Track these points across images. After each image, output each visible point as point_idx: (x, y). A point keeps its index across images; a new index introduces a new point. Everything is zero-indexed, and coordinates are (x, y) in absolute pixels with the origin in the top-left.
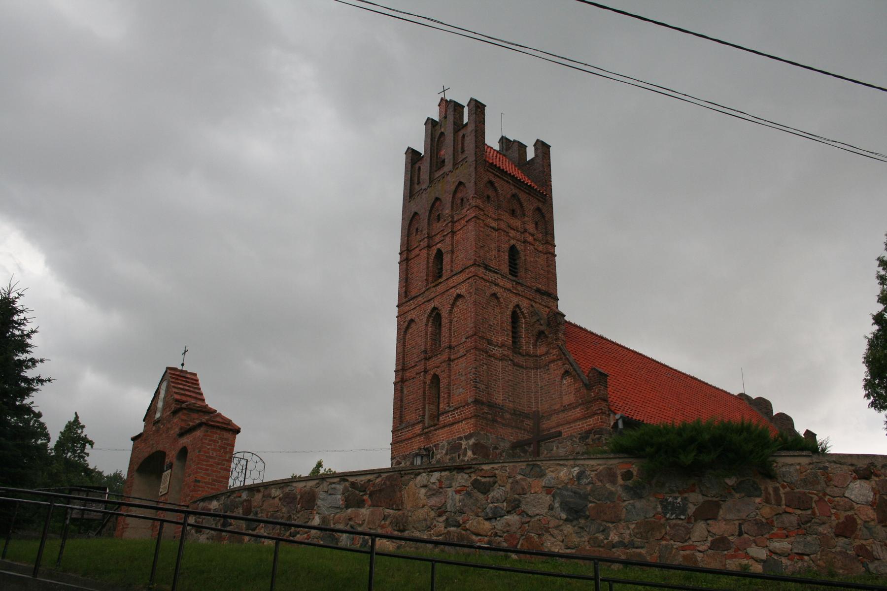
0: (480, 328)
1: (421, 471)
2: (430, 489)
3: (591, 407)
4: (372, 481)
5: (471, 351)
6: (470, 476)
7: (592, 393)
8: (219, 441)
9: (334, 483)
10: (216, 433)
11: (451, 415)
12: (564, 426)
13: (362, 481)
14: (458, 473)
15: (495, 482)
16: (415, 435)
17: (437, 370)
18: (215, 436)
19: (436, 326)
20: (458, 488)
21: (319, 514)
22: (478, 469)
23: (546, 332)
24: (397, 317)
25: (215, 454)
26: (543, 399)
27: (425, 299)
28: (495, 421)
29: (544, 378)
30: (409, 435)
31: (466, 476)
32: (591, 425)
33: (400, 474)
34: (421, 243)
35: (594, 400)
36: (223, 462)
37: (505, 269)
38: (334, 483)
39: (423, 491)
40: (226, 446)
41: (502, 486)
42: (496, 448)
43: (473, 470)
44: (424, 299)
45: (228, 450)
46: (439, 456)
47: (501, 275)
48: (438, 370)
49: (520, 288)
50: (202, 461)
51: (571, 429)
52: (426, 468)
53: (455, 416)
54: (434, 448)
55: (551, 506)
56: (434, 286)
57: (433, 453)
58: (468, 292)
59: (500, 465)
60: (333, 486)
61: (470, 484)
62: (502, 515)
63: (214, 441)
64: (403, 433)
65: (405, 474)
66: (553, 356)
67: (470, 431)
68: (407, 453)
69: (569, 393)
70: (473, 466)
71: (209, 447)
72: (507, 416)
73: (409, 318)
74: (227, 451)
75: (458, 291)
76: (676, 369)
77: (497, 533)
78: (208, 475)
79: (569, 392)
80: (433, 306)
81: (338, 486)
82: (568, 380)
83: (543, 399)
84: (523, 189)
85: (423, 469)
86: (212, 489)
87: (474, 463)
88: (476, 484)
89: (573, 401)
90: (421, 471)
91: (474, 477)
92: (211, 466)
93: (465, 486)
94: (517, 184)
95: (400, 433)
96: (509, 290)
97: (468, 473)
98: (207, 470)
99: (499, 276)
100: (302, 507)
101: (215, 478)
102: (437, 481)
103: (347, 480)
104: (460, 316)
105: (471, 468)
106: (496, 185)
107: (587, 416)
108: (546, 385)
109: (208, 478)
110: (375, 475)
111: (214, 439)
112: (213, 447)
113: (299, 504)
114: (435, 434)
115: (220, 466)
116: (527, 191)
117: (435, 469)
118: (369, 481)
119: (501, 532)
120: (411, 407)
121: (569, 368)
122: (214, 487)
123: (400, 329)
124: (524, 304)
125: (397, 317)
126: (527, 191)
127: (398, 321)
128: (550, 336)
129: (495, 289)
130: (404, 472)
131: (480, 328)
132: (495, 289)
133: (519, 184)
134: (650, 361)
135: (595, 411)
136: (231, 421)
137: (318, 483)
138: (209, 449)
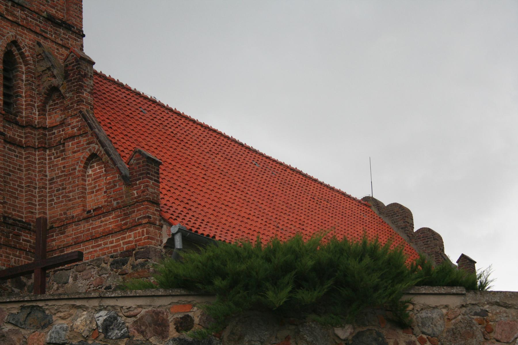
3: (131, 213)
7: (135, 192)
12: (86, 243)
23: (61, 89)
26: (53, 200)
29: (57, 165)
32: (129, 242)
35: (137, 202)
49: (19, 13)
51: (98, 249)
66: (72, 128)
69: (97, 191)
76: (270, 156)
79: (97, 188)
82: (96, 170)
83: (53, 200)
89: (103, 204)
107: (124, 227)
121: (98, 150)
128: (67, 95)
134: (278, 166)
135: (138, 219)
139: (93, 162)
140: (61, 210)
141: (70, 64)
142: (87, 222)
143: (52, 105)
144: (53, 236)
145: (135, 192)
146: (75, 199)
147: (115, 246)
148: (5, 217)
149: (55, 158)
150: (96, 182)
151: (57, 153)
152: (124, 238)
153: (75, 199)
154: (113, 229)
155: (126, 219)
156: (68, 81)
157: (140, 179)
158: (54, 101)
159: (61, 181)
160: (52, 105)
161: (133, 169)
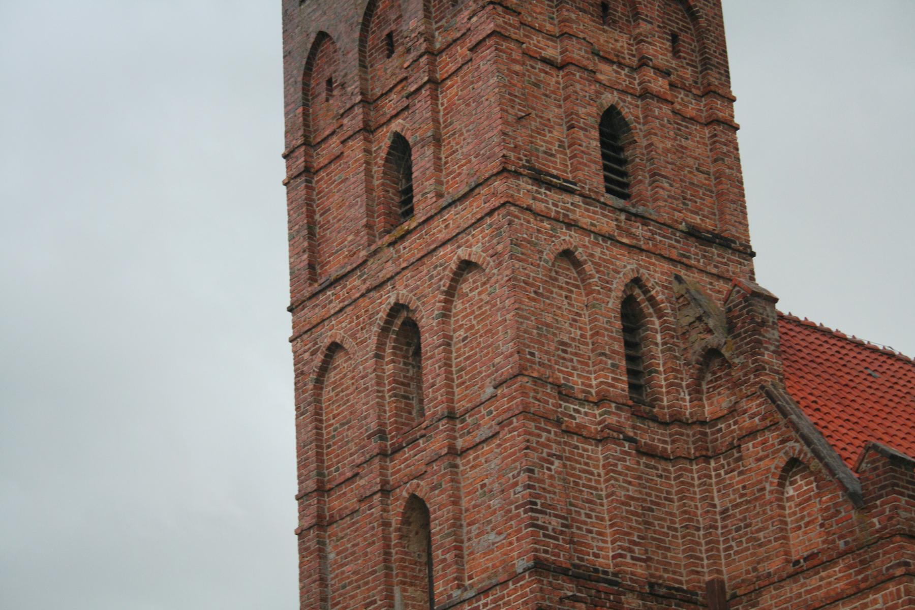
3: (873, 558)
5: (511, 423)
7: (875, 520)
17: (418, 485)
19: (405, 357)
23: (723, 351)
24: (291, 341)
26: (731, 547)
27: (368, 283)
29: (731, 485)
35: (881, 538)
44: (364, 281)
47: (582, 195)
48: (422, 483)
49: (639, 230)
58: (490, 252)
66: (751, 418)
73: (327, 341)
75: (463, 253)
79: (807, 519)
80: (392, 300)
82: (801, 487)
83: (731, 547)
89: (821, 547)
99: (577, 199)
107: (863, 586)
108: (736, 506)
120: (353, 597)
121: (800, 452)
123: (302, 373)
125: (291, 341)
127: (295, 352)
128: (736, 361)
129: (569, 238)
131: (532, 354)
132: (569, 238)
135: (888, 569)
139: (795, 474)
140: (747, 564)
141: (735, 306)
142: (795, 582)
146: (770, 541)
148: (651, 585)
149: (726, 473)
150: (802, 510)
151: (729, 464)
153: (770, 541)
154: (843, 590)
155: (864, 570)
156: (735, 337)
157: (881, 496)
158: (714, 373)
159: (741, 513)
161: (867, 479)
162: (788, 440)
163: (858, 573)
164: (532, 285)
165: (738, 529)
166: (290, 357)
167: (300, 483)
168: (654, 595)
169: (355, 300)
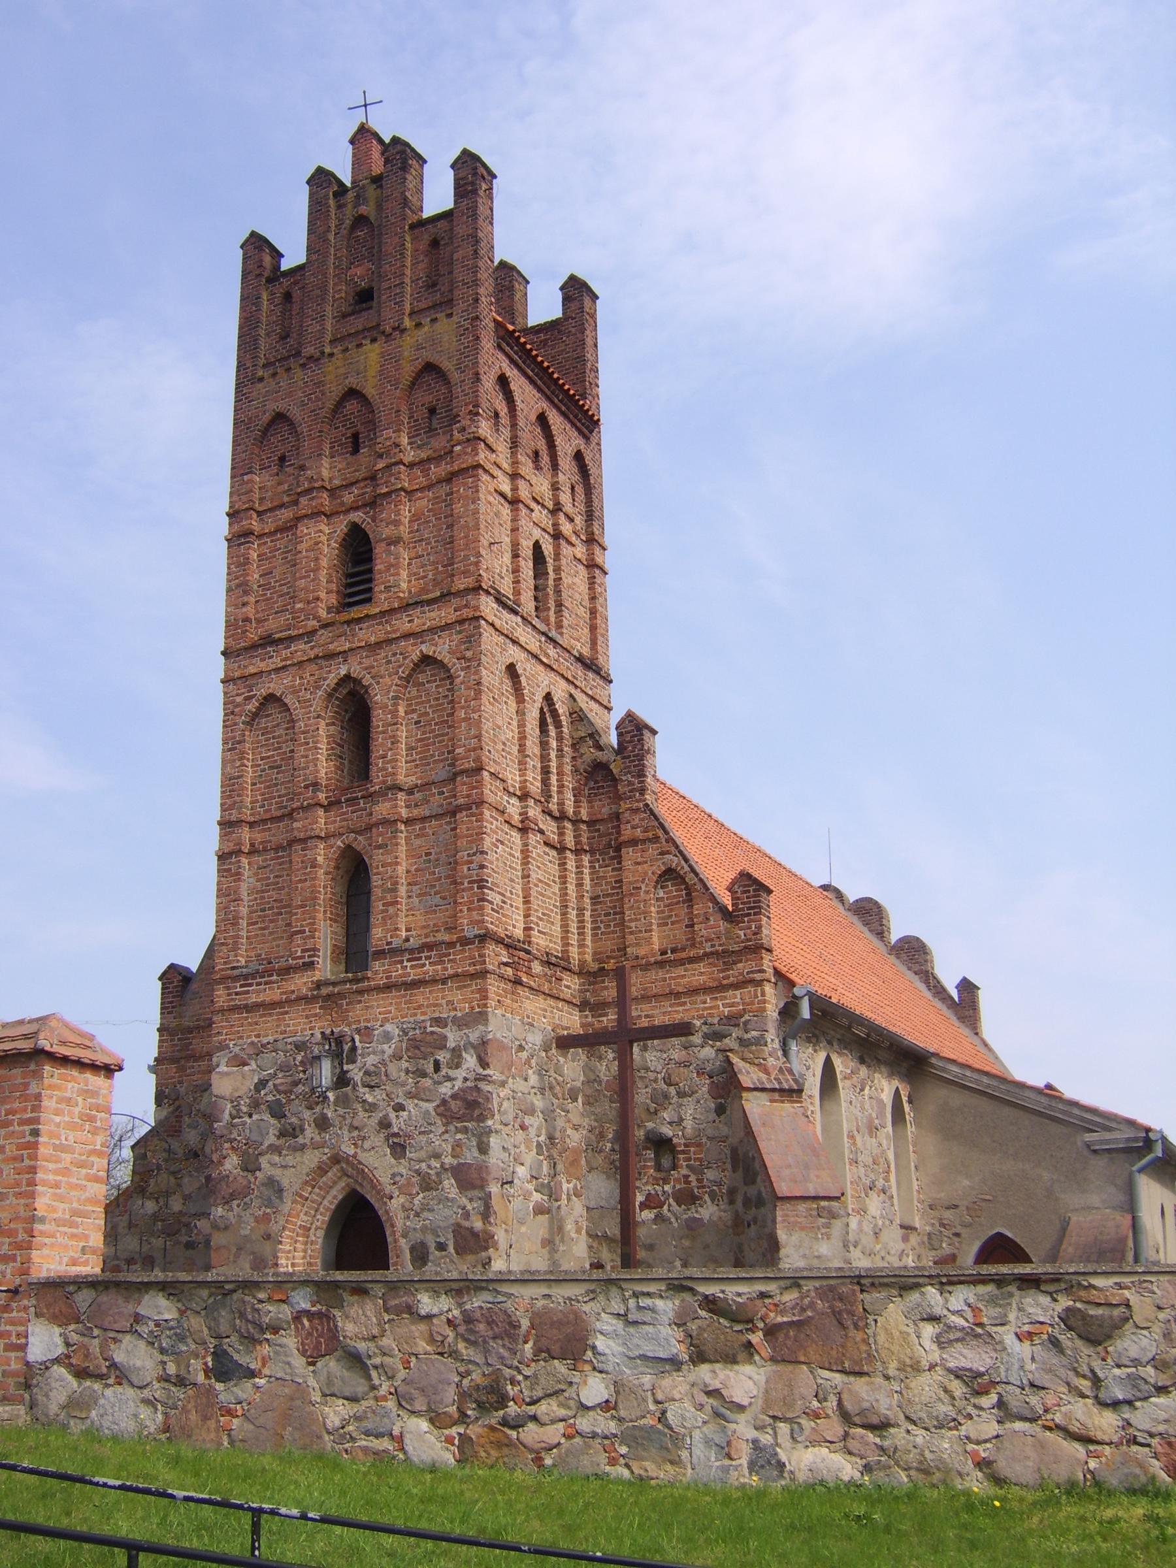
0: (489, 751)
1: (921, 1280)
2: (950, 1328)
3: (735, 963)
4: (770, 1297)
5: (471, 808)
6: (1055, 1300)
7: (742, 933)
8: (80, 1099)
9: (648, 1294)
10: (74, 1079)
11: (408, 960)
12: (661, 998)
13: (739, 1295)
14: (1019, 1289)
15: (1126, 1320)
16: (293, 997)
17: (356, 839)
18: (70, 1085)
19: (342, 721)
20: (1026, 1328)
21: (601, 1372)
22: (1079, 1284)
23: (612, 767)
24: (223, 682)
25: (71, 1138)
26: (599, 928)
27: (316, 651)
28: (518, 982)
29: (605, 878)
30: (273, 994)
31: (1045, 1300)
32: (732, 1005)
33: (858, 1283)
34: (302, 500)
35: (745, 947)
36: (92, 1159)
37: (528, 605)
38: (648, 1294)
39: (929, 1330)
40: (94, 1113)
41: (1142, 1328)
42: (521, 1048)
43: (1063, 1286)
44: (312, 648)
45: (99, 1124)
46: (371, 1060)
47: (522, 617)
48: (360, 838)
49: (552, 651)
50: (47, 1161)
51: (681, 1008)
52: (938, 1276)
53: (424, 965)
54: (357, 1038)
55: (1071, 1322)
56: (348, 622)
57: (354, 1049)
58: (458, 655)
59: (1135, 1278)
60: (645, 1302)
61: (1057, 1319)
62: (1147, 1395)
63: (68, 1101)
64: (250, 985)
65: (873, 1284)
66: (633, 827)
67: (472, 1008)
68: (265, 1041)
69: (673, 923)
70: (1067, 1277)
71: (58, 1119)
72: (537, 968)
73: (264, 692)
74: (97, 1128)
75: (425, 648)
77: (1135, 1437)
78: (61, 1199)
79: (674, 919)
80: (343, 672)
81: (660, 1303)
82: (671, 891)
83: (599, 928)
84: (556, 401)
85: (929, 1277)
86: (73, 1236)
87: (1071, 1270)
88: (1068, 1319)
89: (684, 942)
90: (921, 1280)
91: (1064, 1302)
92: (65, 1172)
93: (1042, 1323)
94: (548, 388)
95: (242, 986)
96: (535, 657)
97: (1051, 1294)
98: (57, 1185)
99: (519, 619)
100: (538, 1351)
101: (75, 1205)
102: (966, 1308)
103: (691, 1290)
104: (430, 711)
105: (1058, 1280)
106: (513, 386)
107: (725, 982)
108: (608, 895)
109: (62, 1206)
110: (782, 1283)
111: (68, 1095)
112: (67, 1119)
113: (526, 1342)
114: (360, 1002)
115: (84, 1171)
116: (563, 408)
117: (962, 1278)
118: (763, 1295)
119: (1146, 1435)
120: (271, 921)
121: (677, 865)
122: (75, 1231)
123: (232, 713)
124: (560, 691)
125: (223, 682)
126: (563, 408)
127: (225, 693)
128: (624, 778)
129: (514, 654)
130: (870, 1280)
131: (489, 751)
132: (514, 654)
133: (553, 387)
135: (748, 973)
136: (92, 1037)
137: (593, 1291)
138: (58, 1125)
139: (667, 880)
140: (613, 944)
141: (628, 732)
142: (662, 968)
143: (593, 788)
144: (603, 981)
145: (742, 933)
146: (641, 931)
147: (710, 1008)
148: (547, 954)
149: (600, 867)
150: (671, 910)
151: (604, 860)
152: (725, 998)
153: (641, 931)
154: (705, 982)
155: (728, 970)
156: (623, 758)
157: (749, 915)
158: (596, 782)
159: (611, 901)
160: (593, 788)
161: (738, 898)
162: (668, 853)
163: (719, 971)
164: (491, 691)
165: (606, 915)
166: (220, 698)
167: (223, 810)
168: (549, 963)
169: (301, 662)
